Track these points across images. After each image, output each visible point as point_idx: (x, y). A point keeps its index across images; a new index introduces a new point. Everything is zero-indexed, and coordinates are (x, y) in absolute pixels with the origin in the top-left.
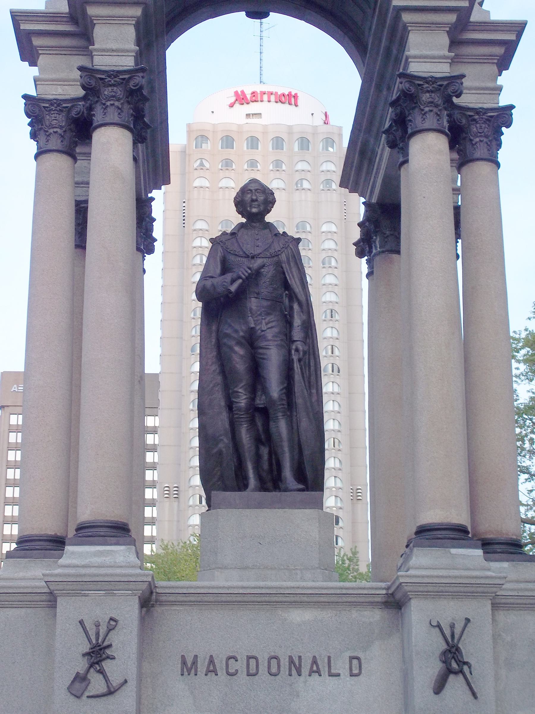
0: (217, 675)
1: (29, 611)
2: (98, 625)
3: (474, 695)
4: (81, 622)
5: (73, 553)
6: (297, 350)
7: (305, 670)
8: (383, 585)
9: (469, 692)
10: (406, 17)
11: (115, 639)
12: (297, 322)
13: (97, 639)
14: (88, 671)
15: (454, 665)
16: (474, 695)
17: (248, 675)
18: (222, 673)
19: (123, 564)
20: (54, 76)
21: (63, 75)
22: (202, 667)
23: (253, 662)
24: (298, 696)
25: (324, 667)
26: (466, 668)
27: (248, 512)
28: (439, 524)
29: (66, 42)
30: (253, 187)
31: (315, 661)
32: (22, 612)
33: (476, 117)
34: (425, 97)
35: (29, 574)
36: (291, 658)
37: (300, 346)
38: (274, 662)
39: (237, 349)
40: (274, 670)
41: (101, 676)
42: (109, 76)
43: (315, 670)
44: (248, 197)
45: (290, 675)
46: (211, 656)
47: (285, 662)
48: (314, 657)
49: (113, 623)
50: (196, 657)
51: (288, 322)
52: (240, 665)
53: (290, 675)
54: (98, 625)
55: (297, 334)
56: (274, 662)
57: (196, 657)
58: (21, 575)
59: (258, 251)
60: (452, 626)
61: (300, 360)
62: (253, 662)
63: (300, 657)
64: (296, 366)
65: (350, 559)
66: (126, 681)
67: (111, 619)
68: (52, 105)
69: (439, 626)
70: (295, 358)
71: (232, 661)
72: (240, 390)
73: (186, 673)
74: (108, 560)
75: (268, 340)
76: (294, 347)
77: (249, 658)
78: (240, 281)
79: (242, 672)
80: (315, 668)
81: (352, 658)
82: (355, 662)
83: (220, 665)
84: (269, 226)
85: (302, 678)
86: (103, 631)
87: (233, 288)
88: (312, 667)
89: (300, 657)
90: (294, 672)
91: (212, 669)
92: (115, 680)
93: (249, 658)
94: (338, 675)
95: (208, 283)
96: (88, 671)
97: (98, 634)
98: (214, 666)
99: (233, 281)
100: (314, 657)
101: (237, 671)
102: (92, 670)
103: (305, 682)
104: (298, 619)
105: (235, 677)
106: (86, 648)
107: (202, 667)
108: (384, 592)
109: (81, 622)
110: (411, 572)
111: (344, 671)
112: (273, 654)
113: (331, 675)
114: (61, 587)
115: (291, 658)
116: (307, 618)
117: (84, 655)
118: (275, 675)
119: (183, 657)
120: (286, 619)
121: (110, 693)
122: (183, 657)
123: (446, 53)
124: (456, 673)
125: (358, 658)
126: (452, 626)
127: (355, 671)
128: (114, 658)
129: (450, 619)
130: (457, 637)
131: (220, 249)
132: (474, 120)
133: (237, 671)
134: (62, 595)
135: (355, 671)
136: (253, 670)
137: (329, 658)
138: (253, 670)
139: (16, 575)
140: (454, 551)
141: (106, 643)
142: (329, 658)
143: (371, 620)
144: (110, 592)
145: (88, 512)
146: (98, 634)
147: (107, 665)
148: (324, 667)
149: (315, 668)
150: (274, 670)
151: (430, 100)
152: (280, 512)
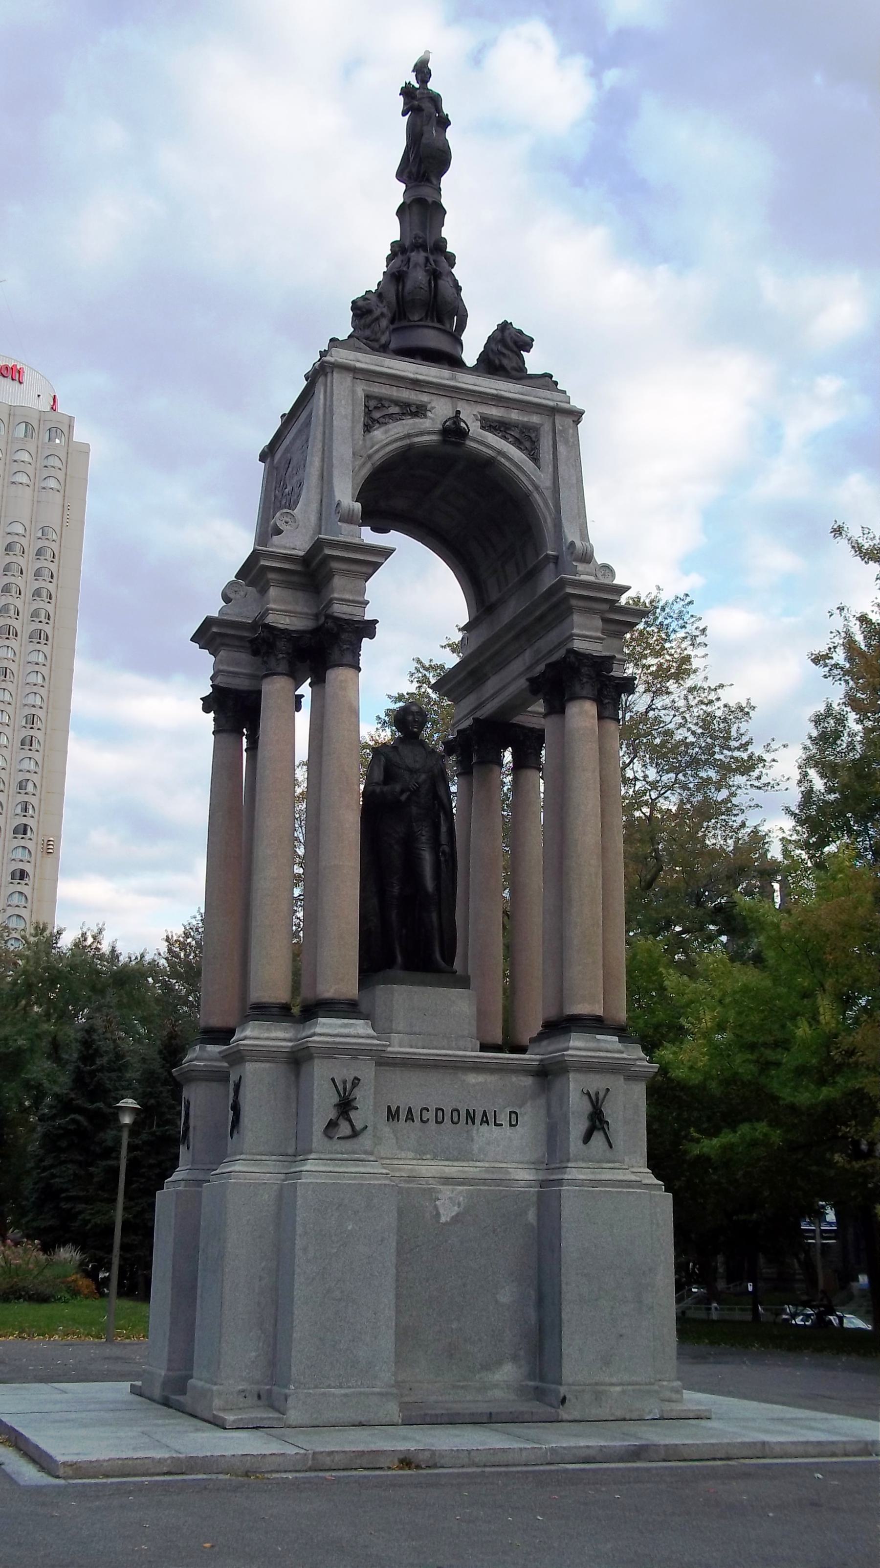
0: (414, 1121)
1: (272, 1065)
2: (345, 1082)
3: (611, 1146)
4: (333, 1080)
5: (324, 1024)
6: (444, 852)
7: (478, 1121)
8: (538, 1057)
9: (606, 1143)
10: (574, 602)
11: (358, 1093)
12: (444, 829)
13: (345, 1093)
14: (338, 1119)
15: (597, 1123)
16: (611, 1146)
17: (437, 1122)
18: (417, 1119)
19: (363, 1035)
20: (283, 608)
21: (289, 608)
22: (403, 1115)
23: (440, 1113)
24: (472, 1140)
25: (491, 1118)
26: (605, 1126)
27: (415, 989)
28: (586, 1015)
29: (295, 579)
30: (414, 708)
31: (485, 1112)
32: (267, 1065)
33: (608, 683)
34: (584, 670)
35: (273, 1035)
36: (467, 1110)
37: (447, 849)
38: (455, 1114)
39: (396, 847)
40: (456, 1119)
41: (348, 1123)
42: (348, 624)
43: (485, 1121)
44: (410, 718)
45: (467, 1123)
46: (410, 1109)
47: (463, 1114)
48: (485, 1111)
49: (357, 1082)
50: (398, 1108)
51: (436, 827)
52: (430, 1115)
53: (467, 1123)
54: (345, 1082)
55: (444, 839)
56: (455, 1114)
57: (398, 1108)
58: (266, 1035)
59: (418, 766)
60: (597, 1094)
61: (446, 861)
62: (440, 1113)
63: (474, 1111)
64: (443, 866)
65: (94, 937)
66: (366, 1127)
67: (356, 1078)
68: (283, 633)
69: (588, 1094)
70: (442, 859)
71: (424, 1112)
72: (395, 882)
73: (391, 1120)
74: (352, 1031)
75: (422, 843)
76: (441, 849)
77: (437, 1110)
78: (408, 793)
79: (432, 1121)
80: (485, 1119)
81: (511, 1113)
82: (513, 1116)
83: (416, 1114)
84: (422, 744)
85: (475, 1127)
86: (348, 1086)
87: (403, 797)
88: (483, 1118)
89: (474, 1111)
90: (470, 1121)
91: (410, 1116)
92: (359, 1126)
93: (437, 1110)
94: (501, 1125)
95: (378, 789)
96: (338, 1119)
97: (345, 1089)
98: (412, 1115)
99: (402, 792)
100: (485, 1111)
101: (428, 1120)
102: (341, 1117)
103: (478, 1129)
104: (474, 1081)
105: (427, 1124)
106: (335, 1100)
107: (403, 1115)
108: (537, 1063)
109: (333, 1080)
110: (570, 1052)
111: (505, 1124)
112: (455, 1107)
113: (496, 1124)
114: (319, 1051)
115: (467, 1110)
116: (480, 1080)
117: (335, 1105)
118: (456, 1123)
119: (389, 1107)
120: (464, 1081)
121: (355, 1134)
122: (389, 1107)
123: (599, 634)
124: (599, 1129)
125: (516, 1113)
126: (597, 1094)
127: (514, 1123)
128: (357, 1108)
129: (595, 1089)
130: (600, 1102)
131: (383, 759)
132: (606, 685)
133: (428, 1120)
134: (318, 1057)
135: (514, 1123)
136: (440, 1120)
137: (495, 1112)
138: (440, 1120)
139: (262, 1036)
140: (598, 1037)
141: (351, 1097)
142: (495, 1112)
143: (526, 1084)
144: (355, 1058)
145: (332, 991)
146: (345, 1089)
147: (353, 1115)
148: (491, 1118)
149: (485, 1119)
150: (456, 1119)
151: (588, 673)
152: (441, 990)
